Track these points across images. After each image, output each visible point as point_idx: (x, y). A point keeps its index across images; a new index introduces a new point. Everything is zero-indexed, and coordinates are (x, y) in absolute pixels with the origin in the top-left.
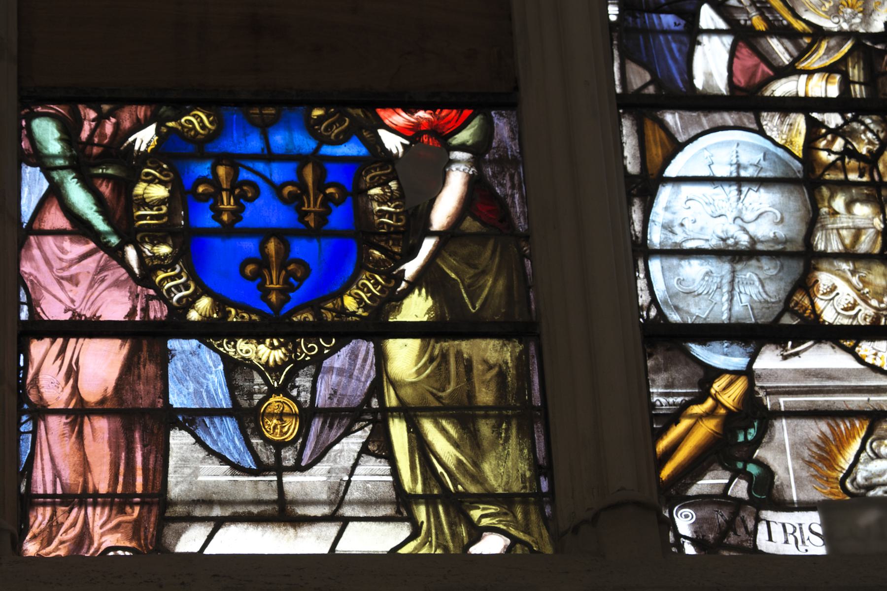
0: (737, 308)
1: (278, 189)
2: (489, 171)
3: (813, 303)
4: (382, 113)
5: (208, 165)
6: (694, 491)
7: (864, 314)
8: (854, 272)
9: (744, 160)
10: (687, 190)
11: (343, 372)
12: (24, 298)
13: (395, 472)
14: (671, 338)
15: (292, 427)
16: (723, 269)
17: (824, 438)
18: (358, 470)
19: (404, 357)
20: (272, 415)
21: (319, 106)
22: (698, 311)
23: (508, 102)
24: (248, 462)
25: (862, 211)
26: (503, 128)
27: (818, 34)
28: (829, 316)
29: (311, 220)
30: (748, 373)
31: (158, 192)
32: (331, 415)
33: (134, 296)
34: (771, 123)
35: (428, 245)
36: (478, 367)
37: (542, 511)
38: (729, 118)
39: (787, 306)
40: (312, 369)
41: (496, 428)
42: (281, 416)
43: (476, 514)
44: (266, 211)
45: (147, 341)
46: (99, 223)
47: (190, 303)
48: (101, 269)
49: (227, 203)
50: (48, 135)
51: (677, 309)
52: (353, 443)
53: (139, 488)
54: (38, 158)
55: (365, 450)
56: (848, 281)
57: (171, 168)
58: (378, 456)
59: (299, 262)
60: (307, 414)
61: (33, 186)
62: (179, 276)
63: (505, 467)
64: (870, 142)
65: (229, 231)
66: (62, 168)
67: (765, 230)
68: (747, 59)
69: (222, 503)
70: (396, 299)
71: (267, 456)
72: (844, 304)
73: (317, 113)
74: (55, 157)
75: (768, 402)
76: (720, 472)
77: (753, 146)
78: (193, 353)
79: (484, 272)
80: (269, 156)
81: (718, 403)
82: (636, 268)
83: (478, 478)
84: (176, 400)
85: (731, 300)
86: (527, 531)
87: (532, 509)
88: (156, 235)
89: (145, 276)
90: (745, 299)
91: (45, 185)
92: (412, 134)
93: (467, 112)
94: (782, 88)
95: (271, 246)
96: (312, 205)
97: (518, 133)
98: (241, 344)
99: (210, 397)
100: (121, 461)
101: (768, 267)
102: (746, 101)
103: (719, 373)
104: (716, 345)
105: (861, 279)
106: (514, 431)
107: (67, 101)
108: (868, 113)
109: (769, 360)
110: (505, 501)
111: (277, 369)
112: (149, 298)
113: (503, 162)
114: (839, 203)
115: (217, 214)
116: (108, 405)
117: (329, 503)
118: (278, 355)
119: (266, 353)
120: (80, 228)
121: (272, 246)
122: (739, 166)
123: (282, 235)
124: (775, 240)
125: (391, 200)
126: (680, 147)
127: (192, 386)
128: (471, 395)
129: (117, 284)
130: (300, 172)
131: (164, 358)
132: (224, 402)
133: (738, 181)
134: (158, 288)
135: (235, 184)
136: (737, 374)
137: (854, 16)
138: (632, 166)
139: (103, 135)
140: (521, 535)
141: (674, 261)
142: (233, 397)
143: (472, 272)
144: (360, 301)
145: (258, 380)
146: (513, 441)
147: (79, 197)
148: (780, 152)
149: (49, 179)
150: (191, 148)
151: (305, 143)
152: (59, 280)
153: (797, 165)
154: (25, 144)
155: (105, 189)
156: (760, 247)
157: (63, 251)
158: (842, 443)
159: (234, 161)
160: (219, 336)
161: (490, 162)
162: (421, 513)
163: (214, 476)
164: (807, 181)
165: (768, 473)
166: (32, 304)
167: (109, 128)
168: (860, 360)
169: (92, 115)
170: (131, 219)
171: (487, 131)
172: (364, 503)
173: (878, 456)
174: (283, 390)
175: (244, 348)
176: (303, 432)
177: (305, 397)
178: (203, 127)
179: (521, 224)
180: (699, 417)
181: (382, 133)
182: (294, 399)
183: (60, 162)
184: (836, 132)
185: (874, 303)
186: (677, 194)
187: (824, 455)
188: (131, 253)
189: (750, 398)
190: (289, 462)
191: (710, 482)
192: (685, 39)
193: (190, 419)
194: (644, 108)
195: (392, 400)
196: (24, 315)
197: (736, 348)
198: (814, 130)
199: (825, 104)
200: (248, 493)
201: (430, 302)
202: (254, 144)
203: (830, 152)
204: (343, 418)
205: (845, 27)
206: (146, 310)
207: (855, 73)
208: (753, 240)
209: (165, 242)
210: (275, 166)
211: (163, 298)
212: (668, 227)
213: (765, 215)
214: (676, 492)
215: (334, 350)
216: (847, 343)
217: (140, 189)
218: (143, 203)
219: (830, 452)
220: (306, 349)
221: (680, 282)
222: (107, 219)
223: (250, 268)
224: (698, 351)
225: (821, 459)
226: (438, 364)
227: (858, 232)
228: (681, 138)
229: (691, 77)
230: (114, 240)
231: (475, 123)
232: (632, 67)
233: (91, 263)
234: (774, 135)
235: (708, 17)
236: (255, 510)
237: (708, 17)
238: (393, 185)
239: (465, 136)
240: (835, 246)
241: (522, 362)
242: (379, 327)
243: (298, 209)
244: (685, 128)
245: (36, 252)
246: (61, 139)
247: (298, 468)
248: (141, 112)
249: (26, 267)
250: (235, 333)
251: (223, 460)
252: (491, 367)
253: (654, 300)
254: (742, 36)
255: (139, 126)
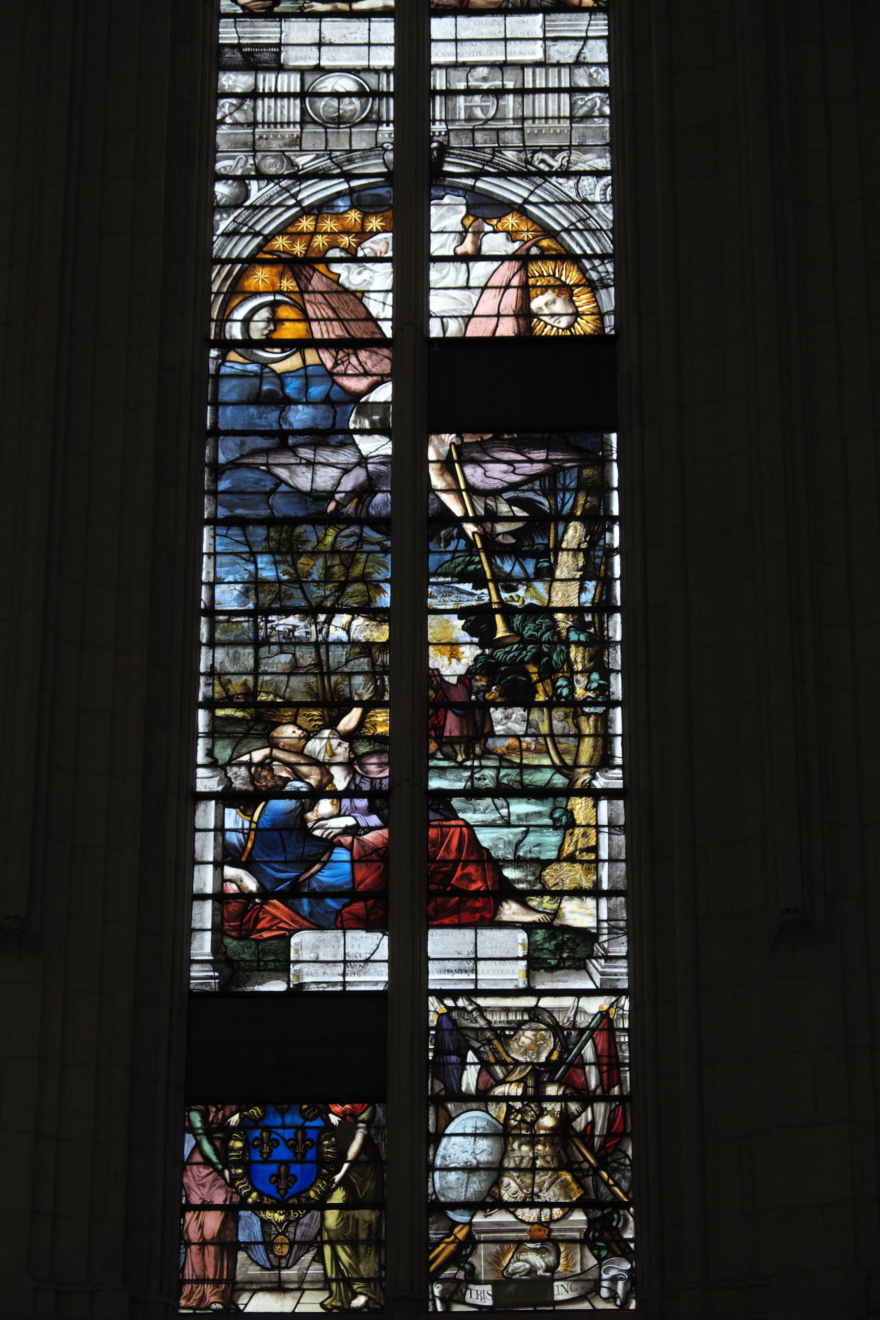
0: (468, 1194)
1: (286, 1142)
2: (373, 1133)
3: (500, 1192)
4: (331, 1106)
5: (259, 1131)
6: (442, 1276)
7: (521, 1195)
8: (518, 1177)
9: (479, 1125)
10: (454, 1139)
11: (308, 1223)
12: (184, 1194)
13: (325, 1269)
14: (440, 1208)
15: (286, 1249)
16: (463, 1176)
17: (498, 1252)
18: (311, 1268)
19: (332, 1218)
20: (278, 1244)
21: (305, 1104)
22: (452, 1196)
23: (382, 1100)
24: (268, 1265)
25: (525, 1148)
26: (380, 1111)
27: (517, 1063)
28: (506, 1197)
29: (299, 1156)
30: (470, 1224)
31: (239, 1144)
32: (301, 1243)
33: (227, 1192)
34: (492, 1107)
35: (346, 1166)
36: (361, 1222)
37: (381, 1285)
38: (474, 1105)
39: (489, 1193)
40: (294, 1224)
41: (366, 1250)
42: (282, 1244)
43: (355, 1287)
44: (282, 1152)
45: (231, 1212)
46: (214, 1159)
47: (248, 1195)
48: (215, 1180)
49: (266, 1149)
50: (196, 1119)
51: (444, 1195)
52: (308, 1257)
53: (225, 1277)
54: (192, 1130)
55: (313, 1260)
56: (515, 1181)
57: (245, 1133)
58: (318, 1262)
59: (293, 1176)
60: (292, 1244)
61: (189, 1142)
62: (245, 1183)
63: (368, 1267)
64: (532, 1116)
65: (266, 1161)
66: (201, 1134)
67: (483, 1158)
68: (485, 1076)
69: (257, 1283)
70: (329, 1192)
71: (275, 1263)
72: (512, 1191)
73: (305, 1106)
74: (199, 1128)
75: (476, 1237)
76: (454, 1268)
77: (483, 1118)
78: (249, 1217)
79: (367, 1179)
80: (284, 1127)
81: (456, 1237)
82: (428, 1177)
83: (357, 1271)
84: (241, 1238)
85: (466, 1191)
86: (375, 1294)
87: (378, 1284)
88: (237, 1164)
89: (231, 1184)
90: (472, 1190)
91: (194, 1142)
92: (342, 1116)
93: (366, 1105)
94: (499, 1091)
95: (282, 1168)
96: (300, 1150)
97: (386, 1114)
98: (268, 1213)
99: (255, 1237)
100: (219, 1267)
101: (483, 1175)
102: (482, 1097)
103: (458, 1223)
104: (458, 1211)
105: (521, 1180)
106: (373, 1251)
107: (204, 1101)
108: (533, 1102)
109: (479, 1218)
110: (367, 1281)
111: (280, 1224)
112: (233, 1193)
113: (380, 1128)
114: (516, 1145)
115: (262, 1154)
116: (215, 1241)
117: (297, 1282)
118: (282, 1218)
119: (278, 1217)
120: (207, 1162)
121: (282, 1168)
122: (476, 1128)
123: (286, 1163)
124: (488, 1162)
125: (332, 1146)
126: (452, 1119)
127: (247, 1232)
128: (357, 1235)
129: (220, 1187)
130: (296, 1134)
131: (237, 1219)
132: (260, 1240)
133: (475, 1135)
134: (236, 1188)
135: (270, 1140)
136: (465, 1224)
137: (533, 1054)
138: (432, 1129)
139: (218, 1119)
140: (372, 1296)
141: (445, 1173)
142: (263, 1236)
143: (362, 1179)
144: (316, 1193)
145: (274, 1229)
146: (372, 1255)
147: (207, 1148)
148: (494, 1121)
149: (196, 1139)
150: (253, 1124)
151: (299, 1121)
152: (198, 1185)
153: (501, 1127)
154: (187, 1124)
155: (218, 1144)
156: (481, 1166)
157: (200, 1173)
158: (504, 1254)
159: (268, 1129)
160: (259, 1210)
161: (374, 1127)
162: (334, 1286)
163: (254, 1271)
164: (503, 1135)
165: (473, 1267)
166: (187, 1196)
167: (220, 1116)
168: (516, 1217)
169: (214, 1109)
170: (227, 1157)
171: (374, 1114)
172: (312, 1282)
173: (519, 1260)
174: (283, 1233)
175: (269, 1215)
176: (290, 1252)
177: (291, 1236)
178: (258, 1114)
179: (384, 1157)
180: (448, 1243)
181: (331, 1116)
182: (287, 1237)
183: (200, 1131)
184: (519, 1111)
185: (525, 1191)
186: (449, 1141)
187: (496, 1259)
188: (227, 1173)
189: (469, 1235)
190: (284, 1265)
191: (449, 1272)
192: (460, 1067)
193: (247, 1246)
194: (439, 1102)
195: (326, 1237)
196: (184, 1201)
197: (466, 1213)
198: (510, 1108)
199: (515, 1098)
200: (267, 1278)
201: (344, 1193)
202: (278, 1121)
203: (515, 1121)
204: (305, 1245)
205: (528, 1060)
206: (231, 1198)
207: (530, 1082)
208: (478, 1163)
209: (240, 1168)
210: (286, 1130)
211: (238, 1192)
212: (444, 1158)
213: (484, 1150)
214: (434, 1278)
215: (304, 1215)
216: (512, 1210)
217: (231, 1144)
218: (233, 1149)
219: (499, 1259)
220: (293, 1215)
221: (446, 1182)
222: (218, 1158)
223: (273, 1179)
224: (450, 1214)
225: (496, 1262)
226: (344, 1221)
227: (522, 1158)
228: (454, 1115)
229: (461, 1086)
230: (220, 1167)
231: (369, 1109)
232: (436, 1082)
233: (210, 1178)
234: (492, 1113)
235: (471, 1057)
236: (269, 1286)
237: (471, 1057)
238: (333, 1139)
239: (364, 1116)
240: (512, 1165)
241: (379, 1220)
242: (322, 1205)
243: (294, 1151)
244: (455, 1110)
245: (189, 1173)
246: (201, 1121)
247: (287, 1267)
248: (234, 1108)
249: (185, 1180)
250: (265, 1208)
251: (258, 1264)
252: (366, 1222)
253: (434, 1191)
254: (485, 1066)
255: (233, 1114)
